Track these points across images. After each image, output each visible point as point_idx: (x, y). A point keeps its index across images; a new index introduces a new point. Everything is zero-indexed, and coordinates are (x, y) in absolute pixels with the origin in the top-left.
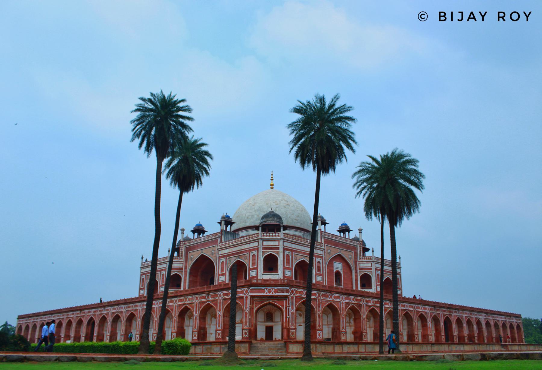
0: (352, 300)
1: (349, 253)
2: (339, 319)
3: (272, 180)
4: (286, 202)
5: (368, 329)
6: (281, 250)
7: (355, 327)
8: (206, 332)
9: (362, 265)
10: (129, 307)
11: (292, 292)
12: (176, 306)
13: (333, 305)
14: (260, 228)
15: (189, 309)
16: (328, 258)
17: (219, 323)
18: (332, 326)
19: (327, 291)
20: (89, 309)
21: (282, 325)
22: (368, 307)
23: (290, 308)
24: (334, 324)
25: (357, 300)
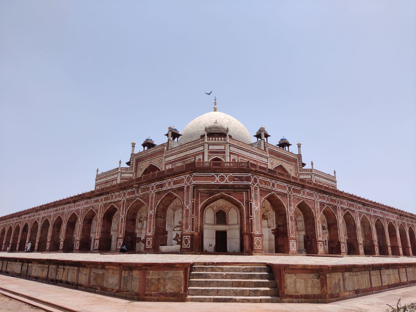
4: (228, 121)
7: (330, 235)
9: (301, 177)
10: (57, 210)
11: (255, 180)
12: (101, 206)
13: (306, 205)
15: (116, 210)
17: (150, 227)
18: (303, 233)
20: (25, 214)
21: (241, 230)
22: (343, 212)
23: (254, 203)
24: (306, 231)
25: (332, 200)
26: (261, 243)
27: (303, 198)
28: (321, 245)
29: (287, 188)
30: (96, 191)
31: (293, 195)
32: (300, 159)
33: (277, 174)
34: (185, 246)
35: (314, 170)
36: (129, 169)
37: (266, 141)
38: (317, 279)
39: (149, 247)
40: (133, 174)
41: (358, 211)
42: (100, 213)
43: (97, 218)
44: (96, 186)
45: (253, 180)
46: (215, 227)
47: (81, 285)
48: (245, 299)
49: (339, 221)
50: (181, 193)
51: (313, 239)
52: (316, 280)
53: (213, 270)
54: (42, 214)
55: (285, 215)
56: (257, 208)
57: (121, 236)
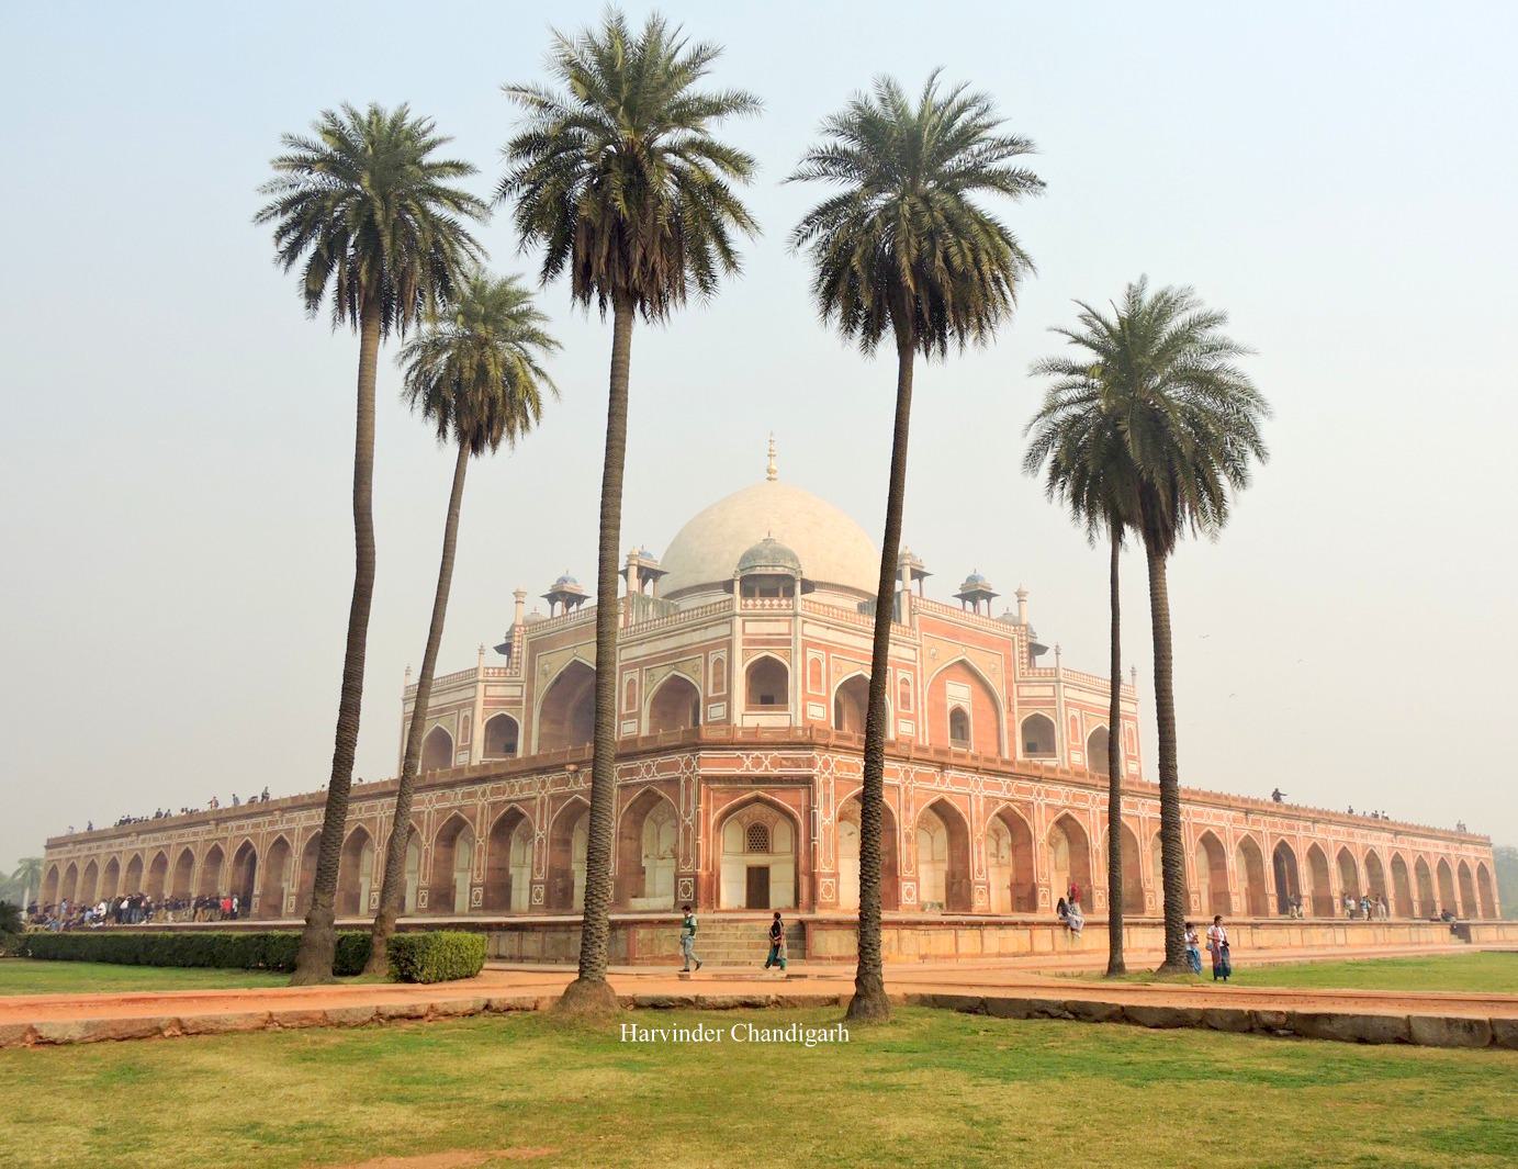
0: (1004, 791)
5: (1053, 874)
7: (1016, 869)
9: (1026, 691)
11: (826, 764)
12: (483, 808)
14: (737, 586)
15: (522, 816)
16: (930, 671)
18: (945, 867)
19: (929, 762)
23: (820, 813)
25: (1019, 790)
26: (833, 890)
30: (467, 771)
32: (1024, 638)
35: (1062, 671)
36: (508, 671)
37: (916, 592)
40: (522, 686)
42: (481, 825)
45: (820, 763)
46: (746, 858)
47: (528, 958)
49: (1038, 837)
51: (964, 881)
57: (539, 878)
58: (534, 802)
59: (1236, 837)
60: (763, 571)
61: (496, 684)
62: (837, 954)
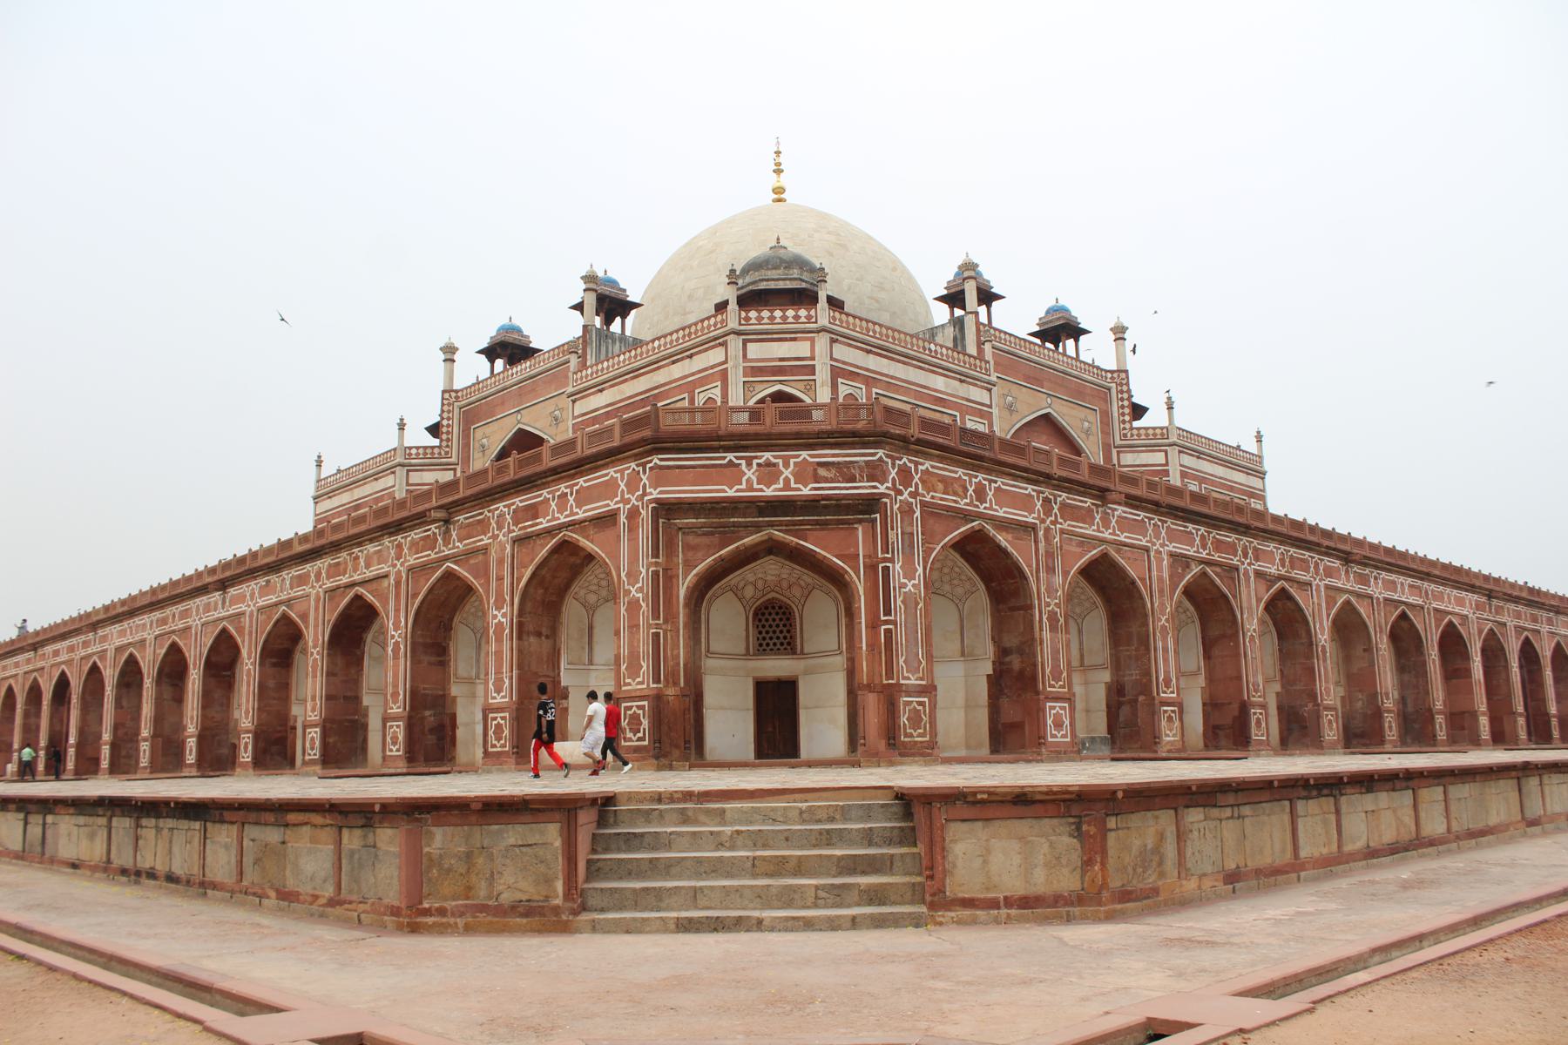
0: (1197, 544)
1: (1082, 413)
2: (1145, 642)
3: (778, 171)
6: (822, 375)
7: (1210, 679)
8: (453, 717)
9: (1128, 459)
10: (164, 621)
12: (317, 600)
13: (1114, 565)
17: (499, 672)
18: (1106, 676)
21: (851, 673)
22: (1262, 588)
24: (1117, 665)
26: (925, 719)
27: (1103, 541)
28: (1170, 719)
29: (1039, 505)
30: (296, 543)
31: (1062, 531)
33: (997, 446)
34: (630, 740)
37: (983, 319)
38: (1071, 835)
39: (498, 746)
41: (1322, 584)
42: (316, 626)
43: (306, 644)
44: (317, 522)
45: (893, 473)
47: (214, 886)
48: (794, 918)
50: (609, 533)
51: (1141, 698)
52: (1066, 839)
53: (685, 818)
54: (116, 637)
55: (1031, 607)
56: (910, 587)
57: (396, 709)
58: (385, 583)
59: (1480, 632)
60: (772, 285)
61: (422, 468)
62: (1017, 888)
